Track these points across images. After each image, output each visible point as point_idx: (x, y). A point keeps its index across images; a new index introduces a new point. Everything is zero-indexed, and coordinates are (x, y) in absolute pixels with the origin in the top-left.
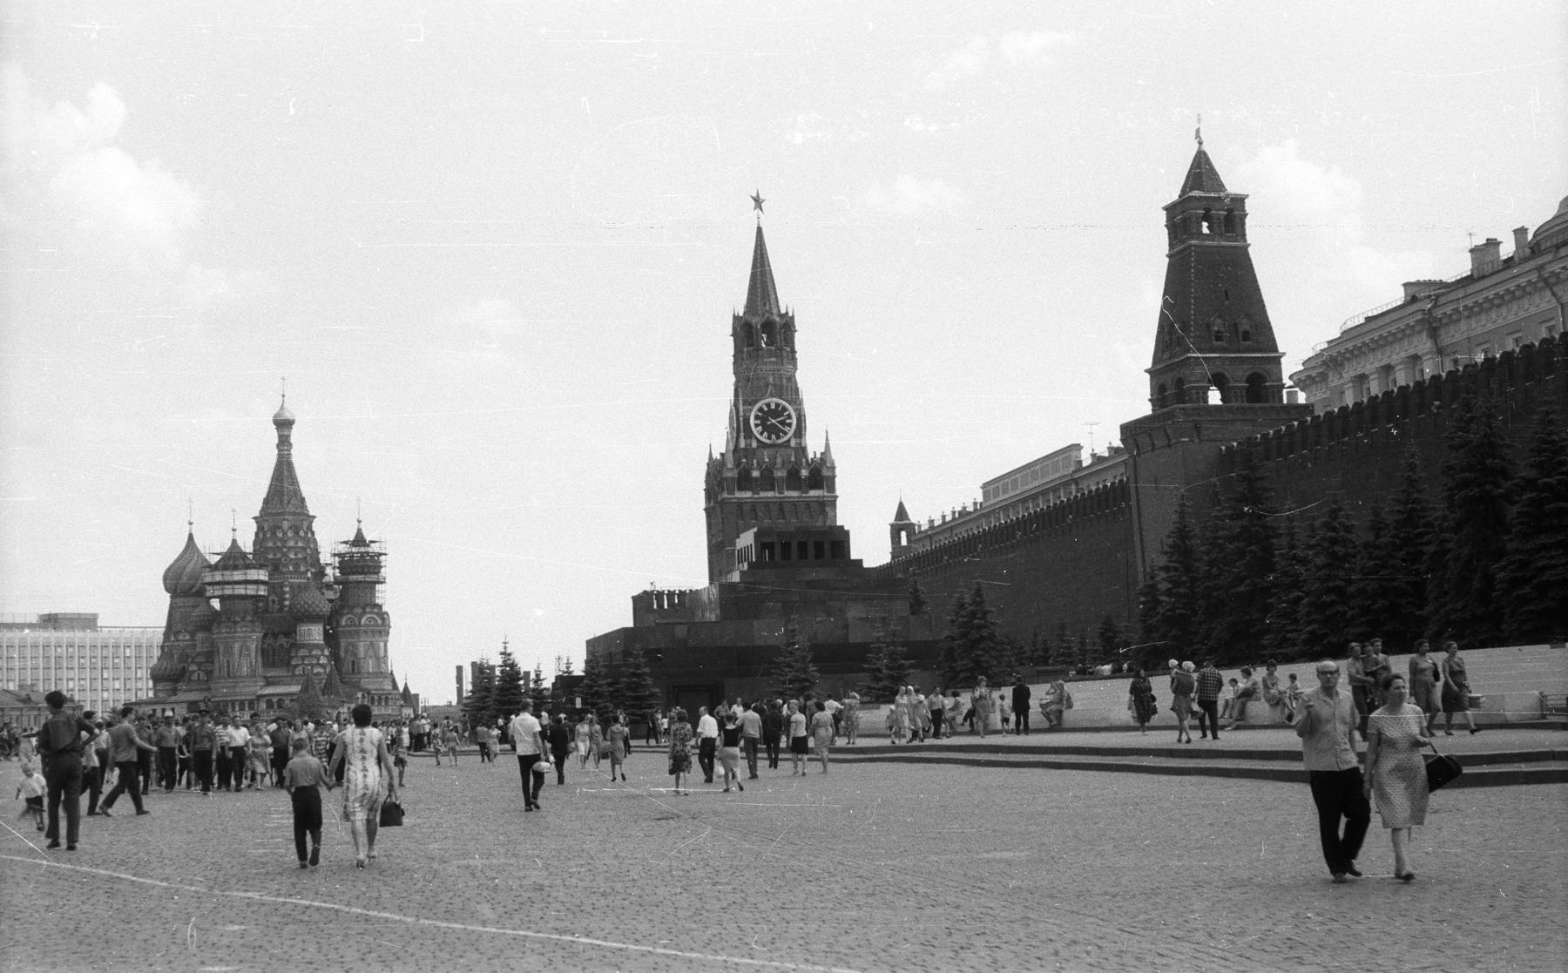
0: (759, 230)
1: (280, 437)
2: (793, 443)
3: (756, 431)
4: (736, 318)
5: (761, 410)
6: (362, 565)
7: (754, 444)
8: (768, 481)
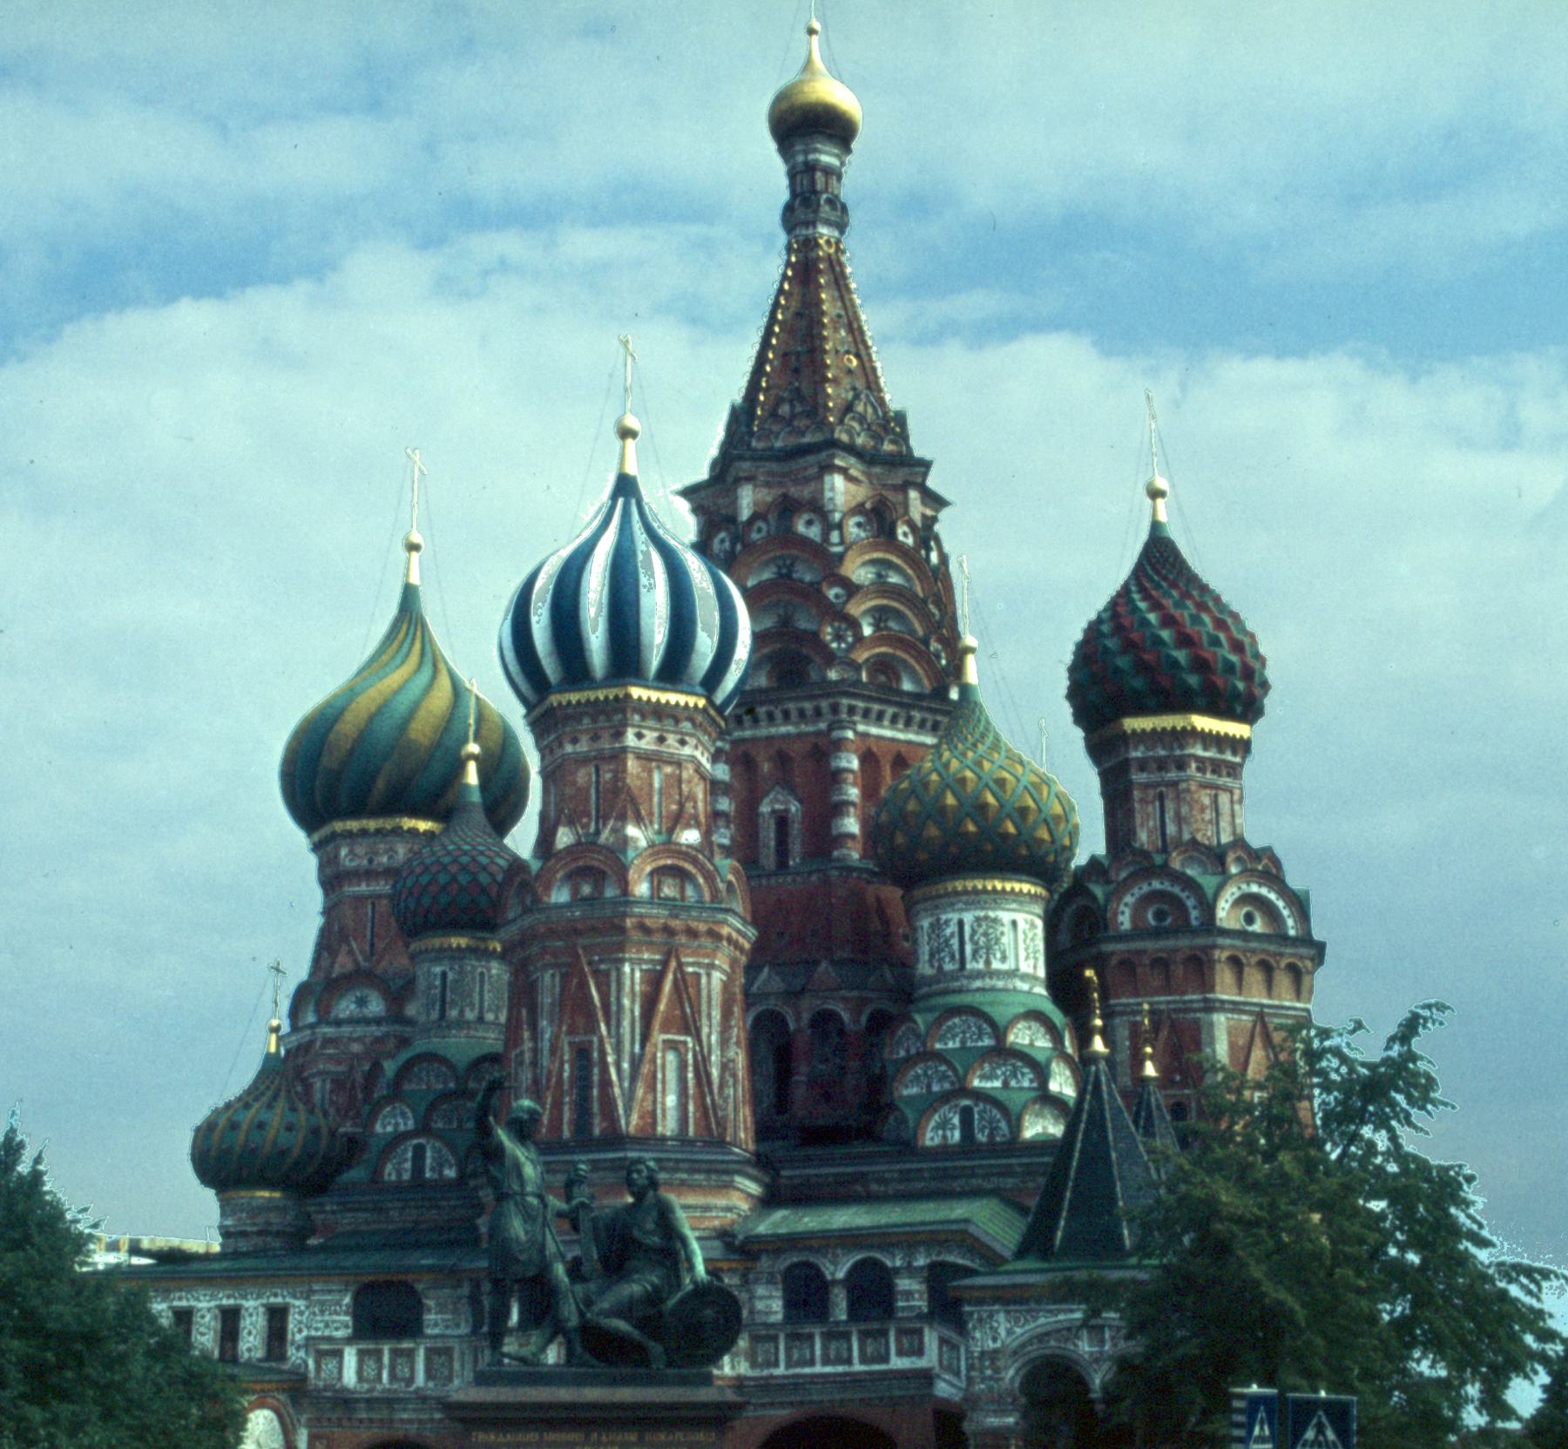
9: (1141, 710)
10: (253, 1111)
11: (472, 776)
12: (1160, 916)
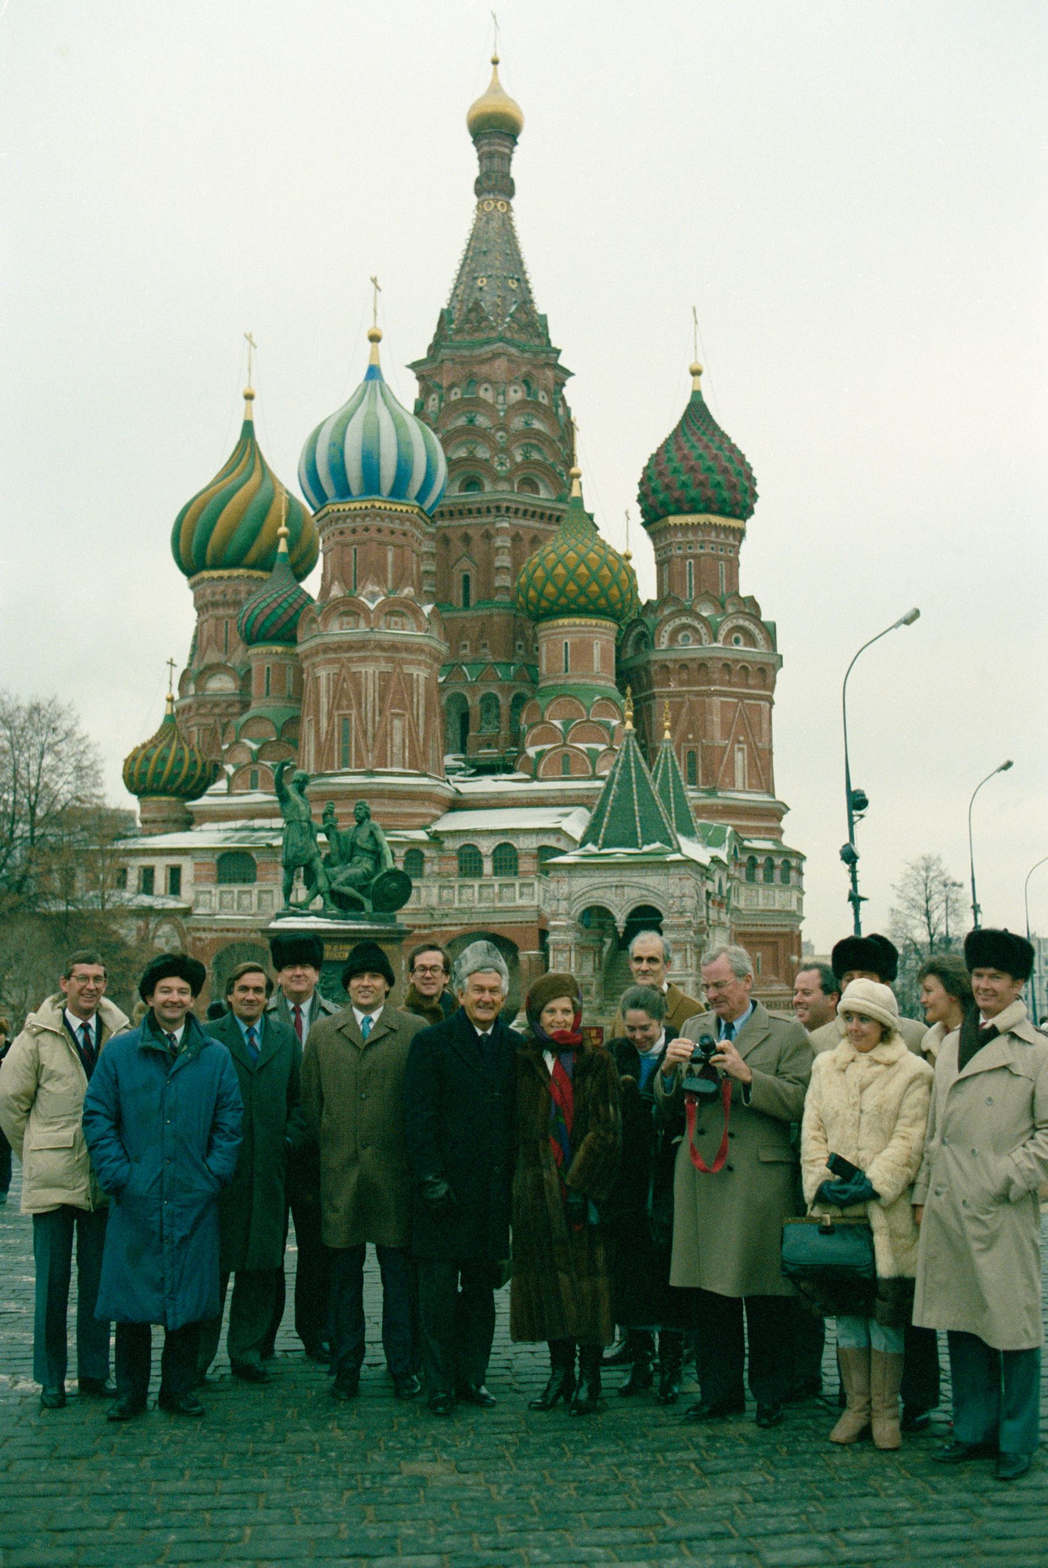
6: (700, 484)
9: (680, 511)
10: (159, 750)
11: (283, 547)
12: (686, 637)
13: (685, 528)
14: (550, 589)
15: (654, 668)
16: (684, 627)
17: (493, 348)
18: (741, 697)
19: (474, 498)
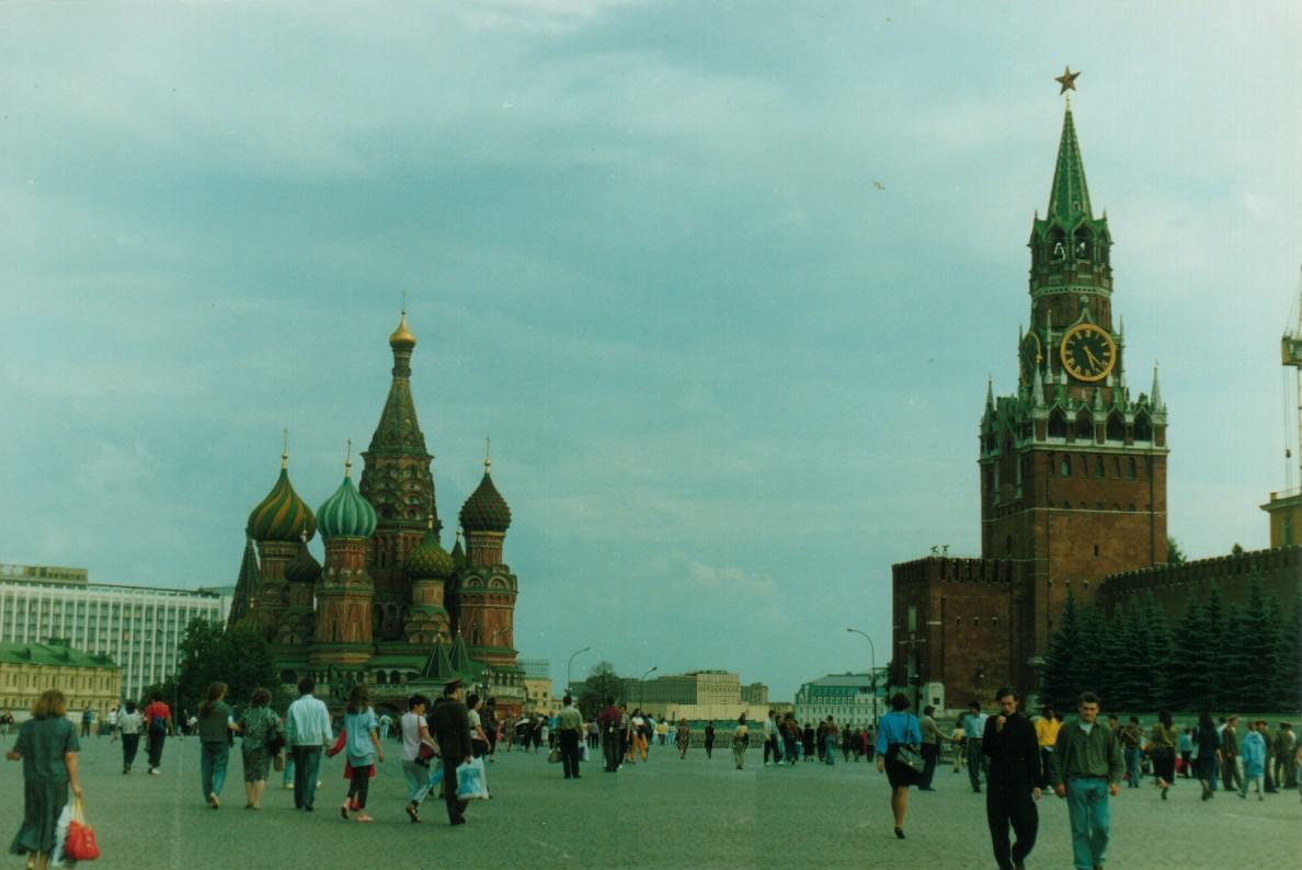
0: (1068, 115)
1: (398, 360)
2: (1110, 382)
3: (1068, 363)
4: (1036, 221)
5: (1073, 337)
6: (485, 513)
7: (1064, 379)
8: (1084, 428)
13: (477, 536)
14: (417, 569)
15: (461, 596)
16: (477, 580)
17: (396, 448)
18: (497, 608)
19: (390, 522)
